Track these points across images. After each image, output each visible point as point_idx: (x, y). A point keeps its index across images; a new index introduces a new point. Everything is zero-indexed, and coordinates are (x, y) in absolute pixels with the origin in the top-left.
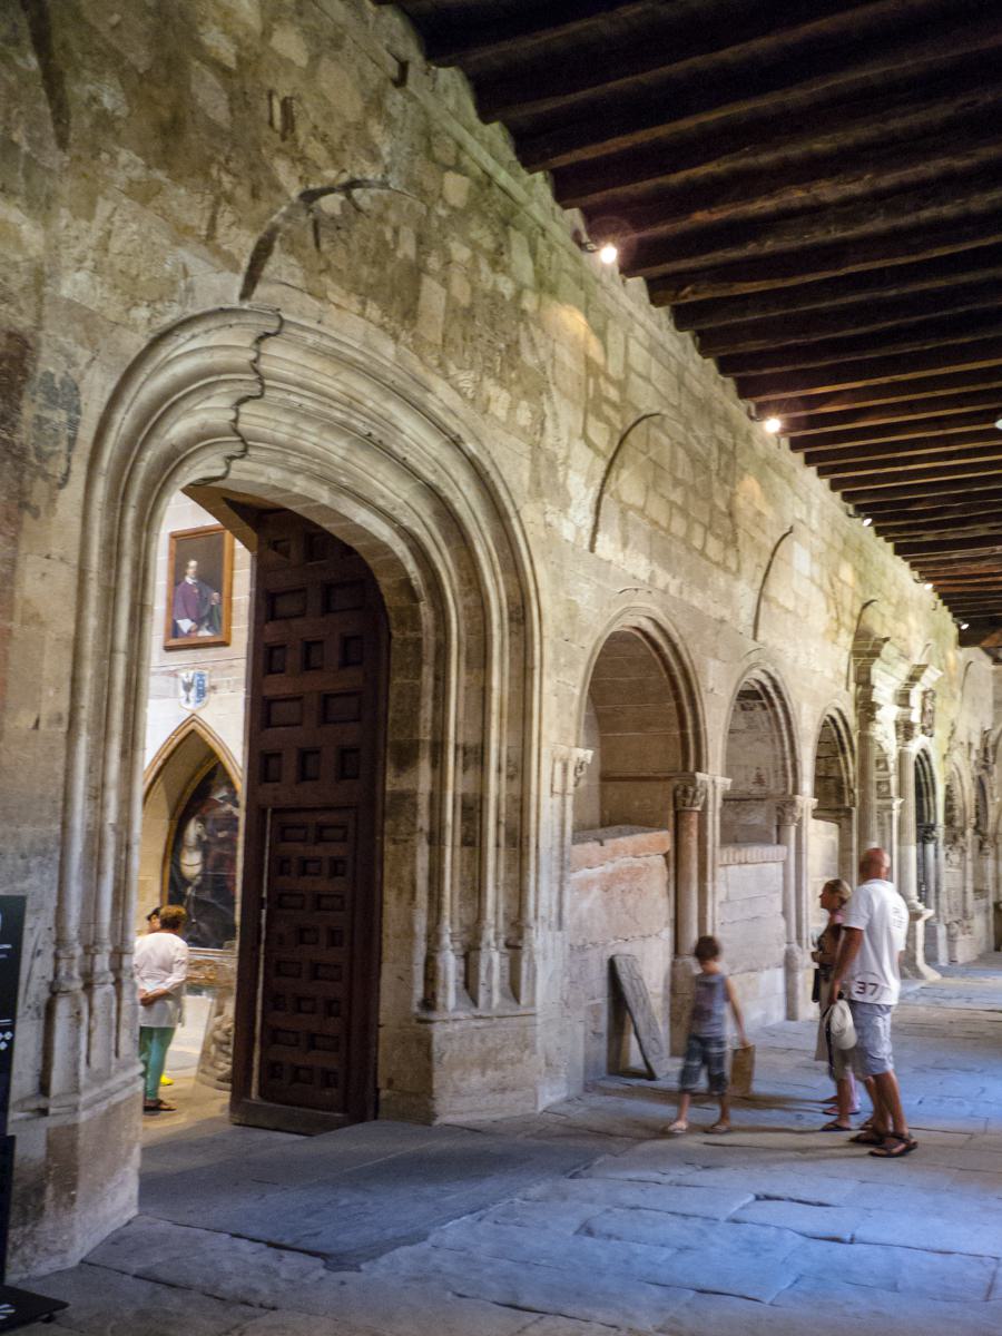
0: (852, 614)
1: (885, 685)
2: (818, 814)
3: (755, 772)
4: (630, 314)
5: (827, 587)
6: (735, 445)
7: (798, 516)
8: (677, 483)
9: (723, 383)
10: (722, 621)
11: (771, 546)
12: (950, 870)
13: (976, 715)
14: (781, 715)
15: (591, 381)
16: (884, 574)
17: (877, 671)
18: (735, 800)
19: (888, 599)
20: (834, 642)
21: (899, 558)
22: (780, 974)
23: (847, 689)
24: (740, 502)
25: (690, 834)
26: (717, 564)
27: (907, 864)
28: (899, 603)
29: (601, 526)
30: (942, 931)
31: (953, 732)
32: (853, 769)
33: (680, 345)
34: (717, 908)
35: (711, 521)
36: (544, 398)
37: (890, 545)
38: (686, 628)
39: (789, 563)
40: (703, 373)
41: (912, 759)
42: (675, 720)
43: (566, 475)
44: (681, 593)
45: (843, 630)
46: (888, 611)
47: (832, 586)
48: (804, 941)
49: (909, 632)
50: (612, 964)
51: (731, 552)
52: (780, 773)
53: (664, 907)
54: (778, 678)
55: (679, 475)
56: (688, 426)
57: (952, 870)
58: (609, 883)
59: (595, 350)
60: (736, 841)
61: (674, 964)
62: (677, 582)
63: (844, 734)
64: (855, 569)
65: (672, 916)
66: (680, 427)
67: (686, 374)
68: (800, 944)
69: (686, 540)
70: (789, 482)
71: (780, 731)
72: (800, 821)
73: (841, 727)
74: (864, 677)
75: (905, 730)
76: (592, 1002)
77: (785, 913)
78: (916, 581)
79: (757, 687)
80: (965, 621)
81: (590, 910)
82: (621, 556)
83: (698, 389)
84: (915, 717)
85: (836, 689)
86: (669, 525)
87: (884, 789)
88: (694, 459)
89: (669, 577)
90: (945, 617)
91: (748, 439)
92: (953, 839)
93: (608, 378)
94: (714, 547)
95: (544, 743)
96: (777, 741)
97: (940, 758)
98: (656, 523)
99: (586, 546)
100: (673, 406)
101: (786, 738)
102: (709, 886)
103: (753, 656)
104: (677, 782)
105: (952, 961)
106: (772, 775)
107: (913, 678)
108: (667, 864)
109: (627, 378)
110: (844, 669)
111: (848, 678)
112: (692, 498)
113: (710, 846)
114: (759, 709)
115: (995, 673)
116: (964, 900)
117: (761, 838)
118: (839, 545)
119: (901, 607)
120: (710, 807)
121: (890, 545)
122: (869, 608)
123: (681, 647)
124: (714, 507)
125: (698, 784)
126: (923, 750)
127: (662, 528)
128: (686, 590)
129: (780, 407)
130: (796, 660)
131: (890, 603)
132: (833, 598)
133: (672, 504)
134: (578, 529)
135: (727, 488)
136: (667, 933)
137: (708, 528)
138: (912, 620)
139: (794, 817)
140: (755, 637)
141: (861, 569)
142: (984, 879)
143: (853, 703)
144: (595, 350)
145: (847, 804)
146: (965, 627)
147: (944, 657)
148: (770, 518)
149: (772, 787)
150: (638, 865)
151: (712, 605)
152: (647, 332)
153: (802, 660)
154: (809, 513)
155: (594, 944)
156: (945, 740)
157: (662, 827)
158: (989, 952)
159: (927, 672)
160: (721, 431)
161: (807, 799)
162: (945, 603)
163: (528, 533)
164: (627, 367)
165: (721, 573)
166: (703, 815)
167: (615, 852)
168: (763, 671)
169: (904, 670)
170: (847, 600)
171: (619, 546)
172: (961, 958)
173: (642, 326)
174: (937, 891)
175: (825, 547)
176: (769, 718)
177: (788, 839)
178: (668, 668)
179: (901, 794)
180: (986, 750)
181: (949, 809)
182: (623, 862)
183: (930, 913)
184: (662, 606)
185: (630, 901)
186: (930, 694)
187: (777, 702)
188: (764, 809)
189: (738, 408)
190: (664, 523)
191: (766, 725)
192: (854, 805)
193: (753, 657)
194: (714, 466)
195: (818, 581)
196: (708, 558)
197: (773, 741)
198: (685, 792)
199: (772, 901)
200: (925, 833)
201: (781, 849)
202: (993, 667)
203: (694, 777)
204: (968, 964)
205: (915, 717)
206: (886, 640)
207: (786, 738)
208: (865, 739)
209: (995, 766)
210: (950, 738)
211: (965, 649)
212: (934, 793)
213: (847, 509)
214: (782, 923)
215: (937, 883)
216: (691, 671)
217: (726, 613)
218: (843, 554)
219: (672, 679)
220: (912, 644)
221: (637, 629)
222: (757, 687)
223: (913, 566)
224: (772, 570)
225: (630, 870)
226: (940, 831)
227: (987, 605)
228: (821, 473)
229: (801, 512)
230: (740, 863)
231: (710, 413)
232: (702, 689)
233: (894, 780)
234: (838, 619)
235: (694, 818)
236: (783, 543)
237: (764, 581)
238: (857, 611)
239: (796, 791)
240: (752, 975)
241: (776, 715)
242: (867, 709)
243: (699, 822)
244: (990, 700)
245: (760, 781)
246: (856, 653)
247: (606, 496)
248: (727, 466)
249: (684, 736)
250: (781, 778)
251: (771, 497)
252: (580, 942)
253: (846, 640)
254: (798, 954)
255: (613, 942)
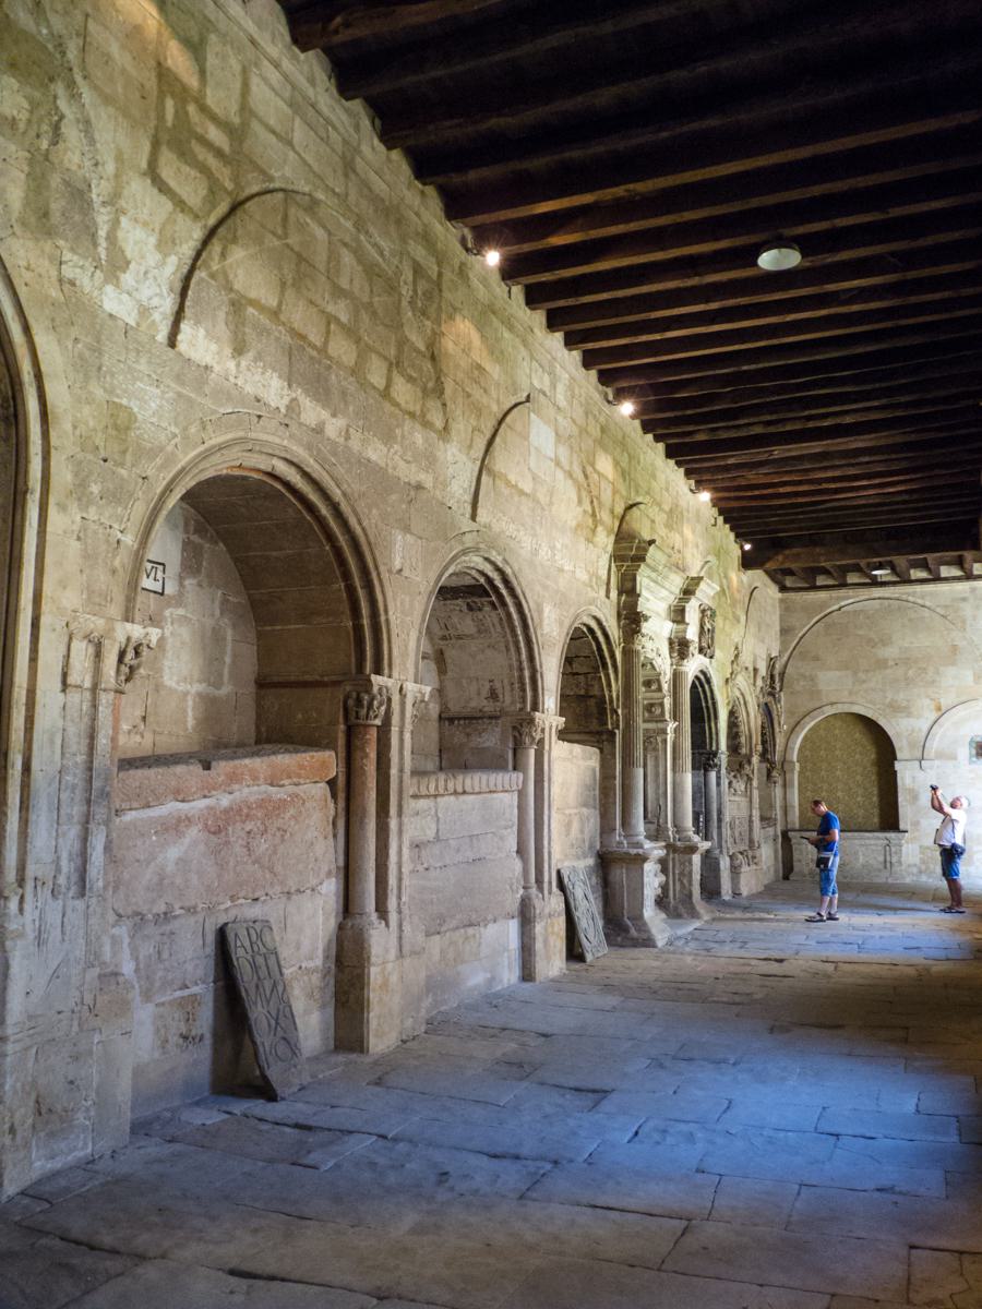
0: (612, 511)
1: (655, 599)
2: (564, 735)
3: (487, 686)
4: (253, 42)
5: (581, 477)
6: (440, 274)
7: (536, 383)
8: (338, 292)
9: (422, 192)
10: (419, 487)
11: (497, 410)
12: (733, 798)
13: (763, 641)
14: (515, 616)
15: (170, 104)
16: (654, 476)
17: (644, 579)
18: (465, 718)
19: (659, 505)
20: (589, 540)
21: (672, 462)
22: (513, 926)
23: (608, 597)
24: (448, 345)
25: (367, 756)
26: (412, 415)
27: (683, 792)
28: (671, 510)
29: (188, 312)
30: (725, 863)
31: (737, 656)
32: (616, 687)
33: (351, 120)
34: (406, 851)
35: (398, 357)
36: (59, 88)
37: (661, 446)
38: (356, 487)
39: (526, 438)
40: (387, 169)
41: (690, 679)
42: (345, 607)
43: (116, 223)
44: (348, 438)
45: (600, 529)
46: (660, 518)
47: (586, 476)
48: (546, 886)
49: (685, 543)
50: (222, 935)
51: (433, 405)
52: (517, 685)
53: (327, 852)
54: (508, 571)
55: (344, 283)
56: (360, 224)
57: (737, 799)
58: (218, 826)
59: (178, 59)
60: (466, 767)
61: (341, 927)
62: (340, 422)
63: (604, 647)
64: (616, 463)
65: (341, 863)
66: (349, 225)
67: (358, 159)
68: (540, 889)
69: (357, 371)
70: (525, 343)
71: (515, 635)
72: (541, 741)
73: (599, 634)
74: (628, 585)
75: (680, 647)
76: (186, 992)
77: (521, 851)
78: (691, 490)
79: (482, 580)
80: (747, 541)
81: (182, 862)
82: (231, 365)
83: (379, 186)
84: (692, 633)
85: (592, 594)
86: (326, 343)
87: (658, 711)
88: (371, 271)
89: (325, 414)
90: (726, 534)
91: (462, 272)
92: (739, 764)
93: (203, 108)
94: (403, 391)
95: (46, 607)
96: (512, 649)
97: (722, 682)
98: (303, 337)
99: (162, 336)
100: (337, 195)
101: (522, 645)
102: (393, 824)
103: (468, 538)
104: (348, 688)
105: (736, 894)
106: (508, 688)
107: (688, 592)
108: (334, 796)
109: (245, 125)
110: (603, 573)
111: (608, 583)
112: (365, 317)
113: (394, 771)
114: (487, 608)
115: (781, 601)
116: (751, 830)
117: (493, 763)
118: (595, 431)
119: (674, 516)
120: (395, 719)
121: (661, 446)
122: (635, 508)
123: (345, 507)
124: (402, 342)
125: (375, 689)
126: (702, 672)
127: (314, 347)
128: (356, 436)
129: (500, 243)
130: (535, 552)
131: (661, 509)
132: (586, 485)
133: (330, 319)
134: (144, 311)
135: (428, 323)
136: (331, 887)
137: (395, 365)
138: (687, 532)
139: (534, 739)
140: (474, 517)
141: (624, 465)
142: (771, 806)
143: (614, 613)
144: (178, 59)
145: (610, 727)
146: (748, 547)
147: (726, 577)
148: (496, 377)
149: (508, 700)
150: (275, 797)
151: (402, 464)
152: (286, 76)
153: (544, 553)
154: (554, 386)
155: (191, 910)
156: (729, 664)
157: (330, 745)
158: (777, 881)
159: (702, 585)
160: (419, 252)
161: (550, 716)
162: (726, 521)
163: (16, 281)
164: (245, 108)
165: (418, 426)
166: (384, 730)
167: (234, 778)
168: (486, 559)
169: (677, 582)
170: (607, 496)
171: (228, 351)
172: (745, 891)
173: (277, 66)
174: (720, 820)
175: (575, 431)
176: (501, 619)
177: (526, 765)
178: (330, 537)
179: (676, 716)
180: (772, 677)
181: (733, 735)
182: (248, 792)
183: (706, 845)
184: (309, 447)
185: (262, 846)
186: (709, 613)
187: (508, 600)
188: (498, 730)
189: (449, 234)
190: (315, 337)
191: (499, 629)
192: (618, 727)
193: (469, 541)
194: (406, 291)
195: (567, 468)
196: (397, 405)
197: (508, 650)
198: (359, 701)
199: (502, 838)
200: (704, 759)
201: (517, 777)
202: (780, 595)
203: (370, 681)
204: (752, 897)
205: (692, 633)
206: (651, 542)
207: (522, 645)
208: (629, 653)
209: (782, 694)
210: (733, 662)
211: (750, 572)
212: (716, 717)
213: (606, 395)
214: (518, 865)
215: (720, 812)
216: (362, 540)
217: (426, 479)
218: (600, 443)
219: (338, 552)
220: (688, 556)
221: (270, 475)
222: (482, 580)
223: (688, 474)
224: (498, 439)
225: (262, 803)
226: (723, 757)
227: (766, 524)
228: (570, 342)
229: (541, 381)
230: (455, 793)
231: (399, 222)
232: (382, 568)
233: (668, 702)
234: (594, 515)
235: (373, 735)
236: (515, 410)
237: (487, 451)
238: (619, 510)
239: (535, 707)
240: (471, 931)
241: (509, 615)
242: (632, 619)
243: (379, 740)
244: (778, 628)
245: (493, 695)
246: (617, 557)
247: (200, 274)
248: (428, 296)
249: (358, 629)
250: (517, 692)
251: (496, 351)
252: (161, 908)
253: (605, 541)
254: (537, 903)
255: (229, 904)
